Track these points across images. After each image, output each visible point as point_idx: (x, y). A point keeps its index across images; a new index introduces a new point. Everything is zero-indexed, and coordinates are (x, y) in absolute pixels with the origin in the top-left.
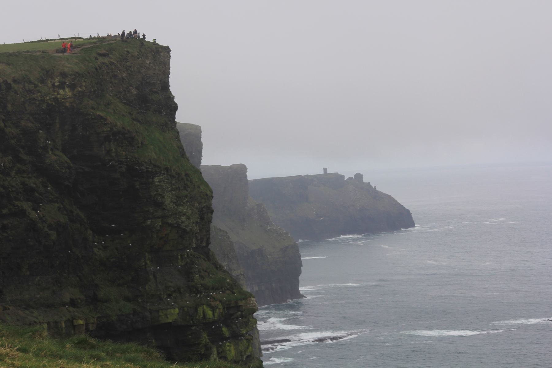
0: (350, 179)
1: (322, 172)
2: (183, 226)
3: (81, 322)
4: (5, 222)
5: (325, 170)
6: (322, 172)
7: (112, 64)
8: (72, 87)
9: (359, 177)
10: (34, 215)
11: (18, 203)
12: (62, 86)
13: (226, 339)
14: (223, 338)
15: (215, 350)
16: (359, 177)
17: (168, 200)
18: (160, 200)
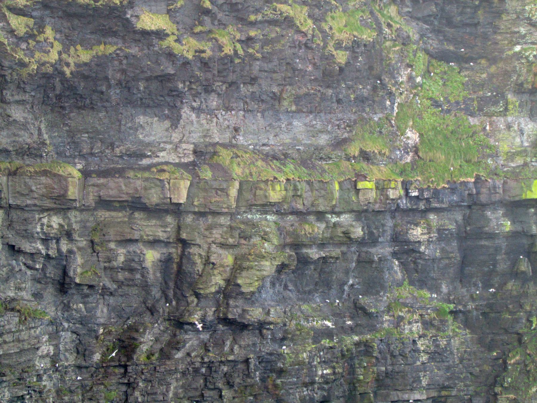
3: (369, 185)
4: (252, 33)
10: (309, 26)
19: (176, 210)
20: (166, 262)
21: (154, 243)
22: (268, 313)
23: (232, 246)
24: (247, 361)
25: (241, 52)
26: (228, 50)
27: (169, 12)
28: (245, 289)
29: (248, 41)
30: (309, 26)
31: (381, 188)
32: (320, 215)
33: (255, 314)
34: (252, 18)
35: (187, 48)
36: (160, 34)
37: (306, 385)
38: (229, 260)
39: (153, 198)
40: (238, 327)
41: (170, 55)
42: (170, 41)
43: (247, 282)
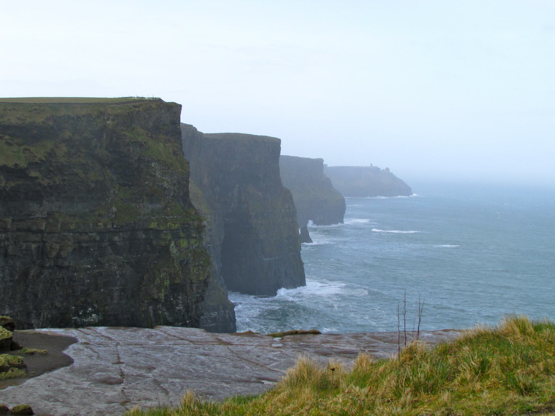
2: (164, 186)
3: (101, 224)
4: (65, 178)
5: (371, 164)
6: (369, 165)
7: (139, 111)
8: (113, 120)
9: (388, 169)
10: (83, 176)
11: (74, 170)
12: (108, 119)
13: (183, 238)
14: (180, 238)
15: (173, 242)
16: (388, 169)
17: (158, 174)
18: (153, 173)
19: (41, 232)
20: (38, 248)
21: (34, 242)
22: (70, 263)
23: (59, 243)
24: (63, 278)
25: (62, 184)
26: (58, 183)
27: (39, 171)
28: (63, 256)
29: (64, 180)
30: (83, 176)
31: (105, 225)
32: (86, 233)
33: (66, 264)
34: (65, 173)
35: (45, 182)
36: (37, 178)
37: (82, 285)
38: (58, 247)
39: (34, 228)
40: (61, 268)
41: (40, 184)
42: (40, 180)
43: (64, 254)
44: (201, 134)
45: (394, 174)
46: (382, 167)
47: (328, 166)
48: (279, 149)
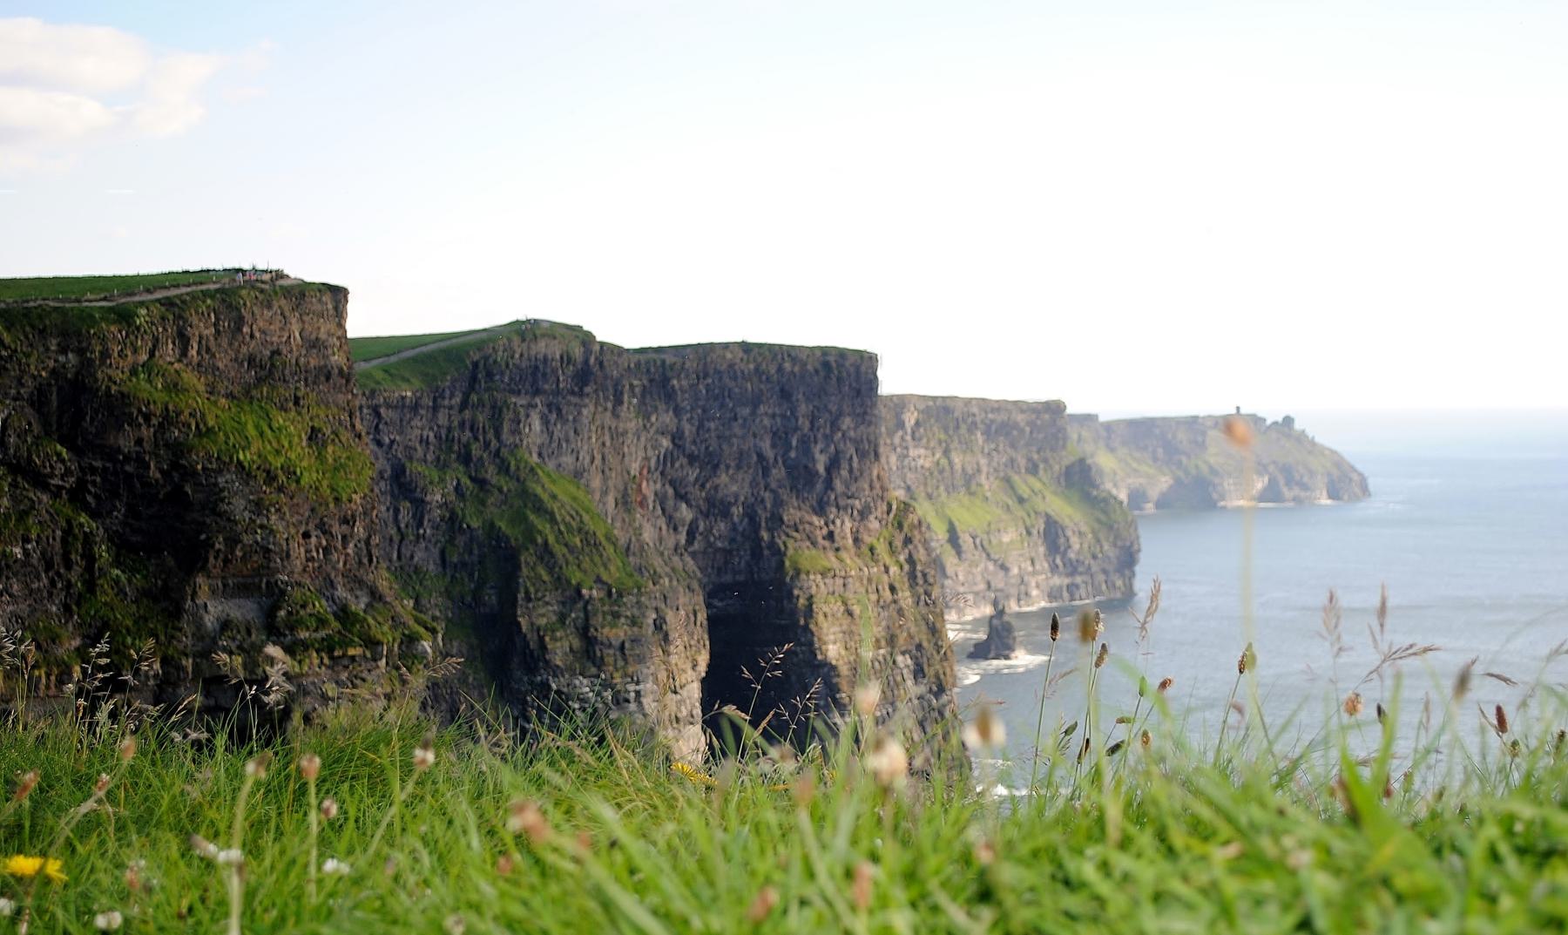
0: (1276, 423)
1: (1234, 411)
6: (1234, 411)
8: (81, 352)
9: (1288, 421)
16: (1288, 421)
44: (620, 351)
45: (1310, 434)
46: (1272, 415)
47: (1102, 419)
48: (873, 382)
